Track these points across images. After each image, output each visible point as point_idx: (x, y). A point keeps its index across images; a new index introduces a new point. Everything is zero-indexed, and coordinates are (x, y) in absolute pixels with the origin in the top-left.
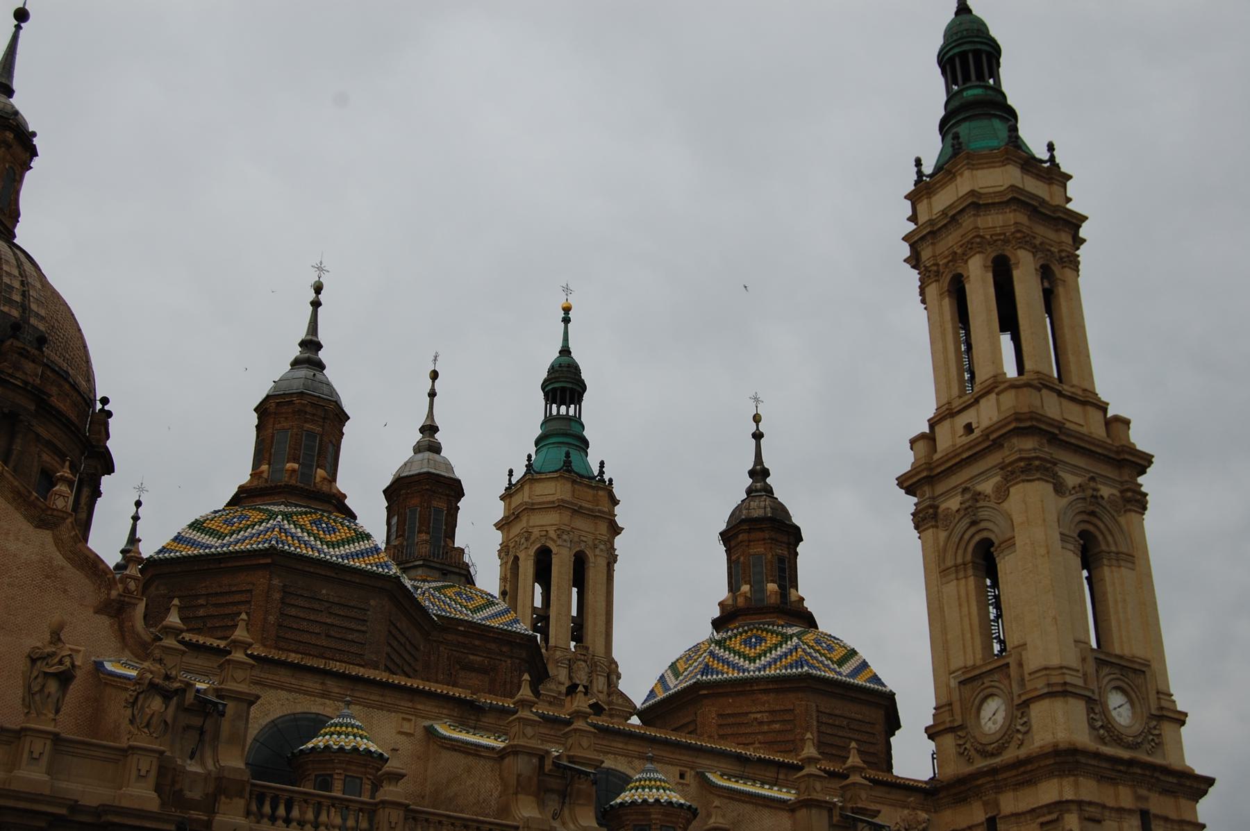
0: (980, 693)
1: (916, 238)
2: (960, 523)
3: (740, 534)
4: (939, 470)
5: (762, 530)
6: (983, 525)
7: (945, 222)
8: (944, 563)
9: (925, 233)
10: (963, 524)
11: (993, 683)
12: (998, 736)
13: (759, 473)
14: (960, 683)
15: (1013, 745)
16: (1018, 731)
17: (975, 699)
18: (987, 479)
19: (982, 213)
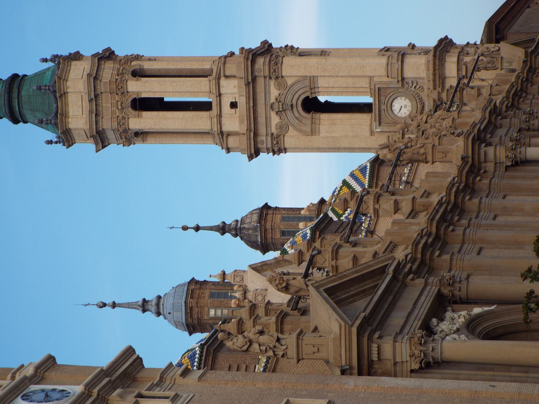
0: (389, 115)
1: (94, 127)
2: (288, 117)
3: (266, 227)
4: (252, 126)
5: (267, 214)
6: (294, 102)
7: (94, 103)
8: (307, 132)
9: (94, 119)
10: (290, 115)
11: (386, 102)
12: (414, 103)
13: (223, 229)
14: (379, 126)
15: (421, 94)
16: (415, 87)
17: (390, 116)
18: (270, 93)
19: (100, 79)
